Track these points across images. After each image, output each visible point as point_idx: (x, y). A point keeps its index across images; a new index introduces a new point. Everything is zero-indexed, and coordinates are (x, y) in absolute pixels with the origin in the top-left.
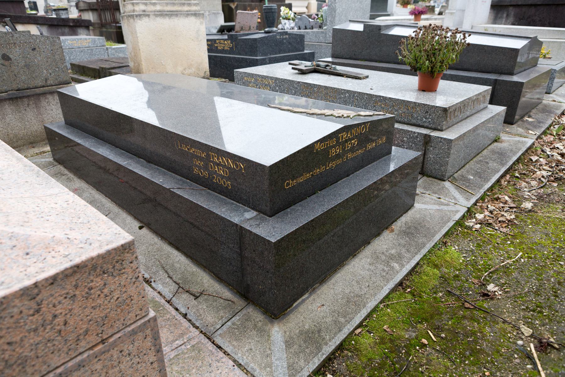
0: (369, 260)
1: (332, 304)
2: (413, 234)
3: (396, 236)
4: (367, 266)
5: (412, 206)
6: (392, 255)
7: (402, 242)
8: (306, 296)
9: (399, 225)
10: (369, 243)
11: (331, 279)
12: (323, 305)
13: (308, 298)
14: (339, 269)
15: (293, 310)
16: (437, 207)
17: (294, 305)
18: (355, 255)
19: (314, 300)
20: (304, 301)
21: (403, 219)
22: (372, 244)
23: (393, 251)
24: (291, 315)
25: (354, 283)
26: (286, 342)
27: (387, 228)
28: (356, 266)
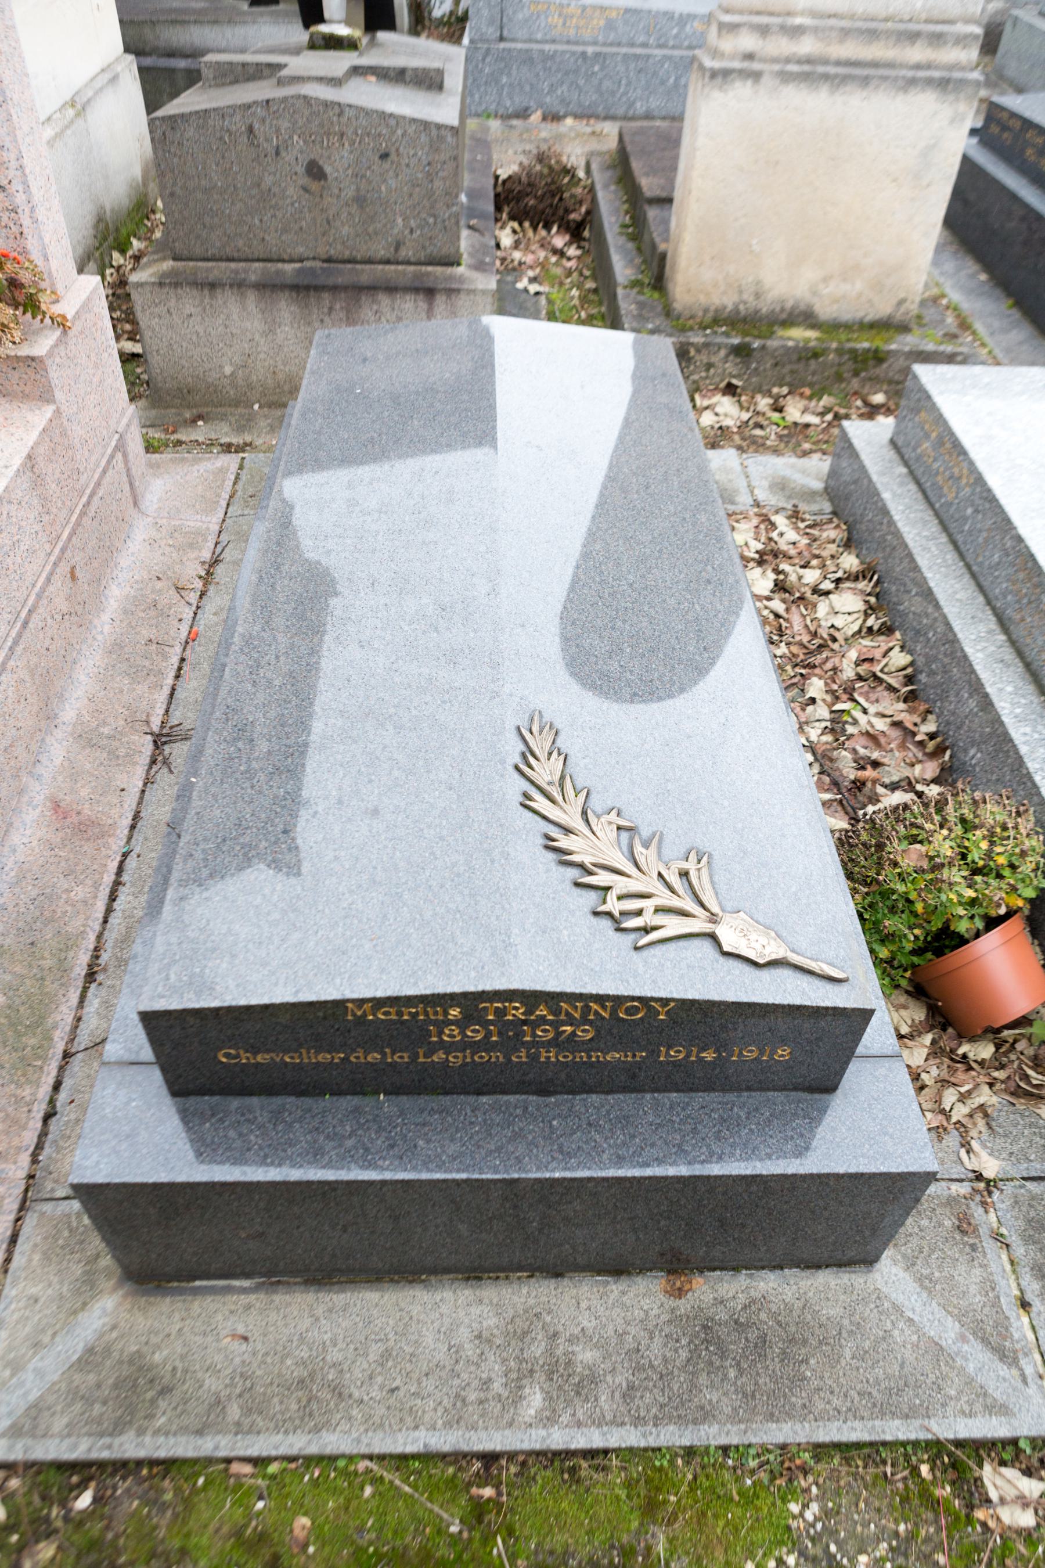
0: (492, 1321)
1: (267, 1354)
2: (723, 1355)
3: (665, 1317)
4: (464, 1334)
5: (869, 1261)
6: (569, 1363)
7: (655, 1351)
8: (246, 1283)
9: (719, 1292)
10: (558, 1275)
11: (343, 1291)
12: (246, 1339)
13: (244, 1291)
14: (392, 1280)
15: (181, 1292)
16: (948, 1331)
17: (198, 1283)
18: (480, 1279)
19: (248, 1307)
20: (229, 1290)
21: (768, 1284)
22: (566, 1281)
23: (586, 1355)
24: (168, 1300)
25: (375, 1351)
26: (90, 1351)
27: (669, 1272)
28: (444, 1309)
